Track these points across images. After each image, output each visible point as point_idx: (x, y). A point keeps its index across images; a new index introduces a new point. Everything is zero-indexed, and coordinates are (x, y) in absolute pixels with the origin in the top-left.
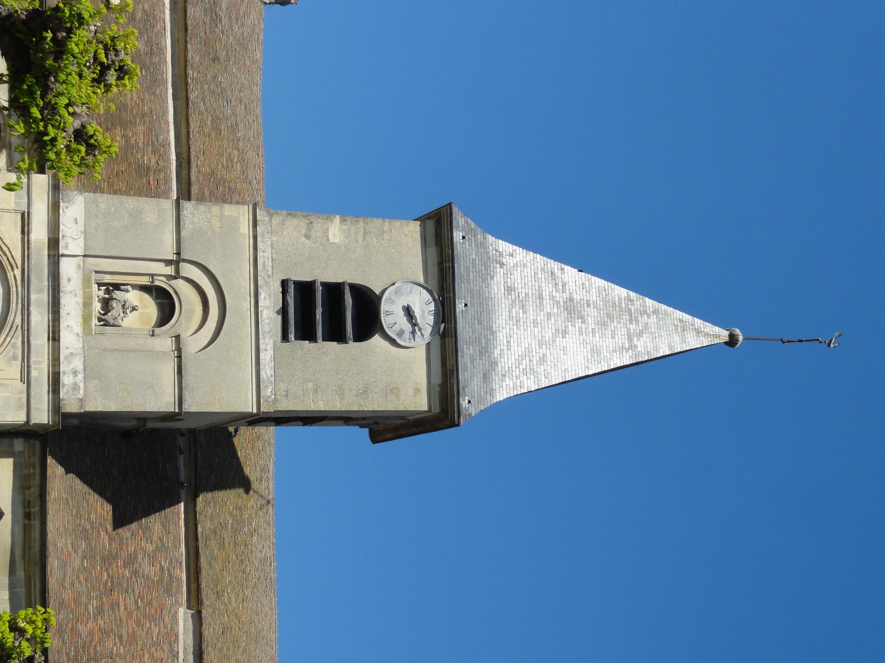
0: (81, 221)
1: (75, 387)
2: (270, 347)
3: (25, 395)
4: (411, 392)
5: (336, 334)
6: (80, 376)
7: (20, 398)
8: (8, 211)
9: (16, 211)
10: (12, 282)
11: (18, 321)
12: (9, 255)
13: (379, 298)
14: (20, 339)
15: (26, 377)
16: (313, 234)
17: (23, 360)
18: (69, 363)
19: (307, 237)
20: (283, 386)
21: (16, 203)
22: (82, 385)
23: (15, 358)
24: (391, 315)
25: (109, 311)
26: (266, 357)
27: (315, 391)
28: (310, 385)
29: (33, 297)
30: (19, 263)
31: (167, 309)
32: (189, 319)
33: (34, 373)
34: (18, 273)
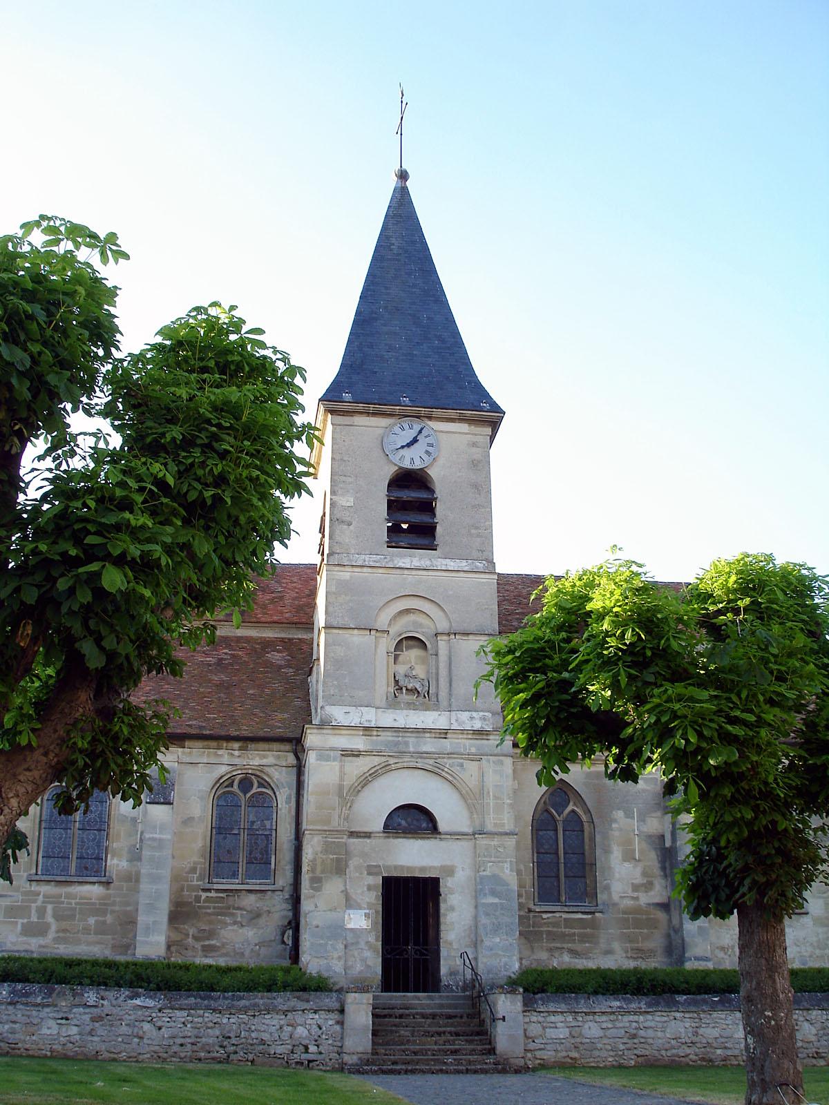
0: (347, 709)
1: (484, 719)
2: (445, 562)
3: (491, 758)
4: (474, 450)
5: (428, 507)
6: (475, 714)
7: (494, 762)
8: (342, 767)
9: (341, 761)
10: (399, 765)
11: (431, 762)
12: (378, 768)
13: (400, 468)
14: (445, 760)
15: (477, 758)
16: (348, 519)
17: (462, 758)
18: (464, 722)
19: (349, 524)
20: (475, 554)
21: (334, 760)
22: (482, 714)
23: (462, 765)
24: (412, 459)
25: (416, 689)
26: (452, 564)
27: (477, 528)
28: (473, 531)
29: (412, 749)
30: (384, 759)
31: (411, 643)
32: (421, 625)
33: (473, 750)
34: (392, 761)
